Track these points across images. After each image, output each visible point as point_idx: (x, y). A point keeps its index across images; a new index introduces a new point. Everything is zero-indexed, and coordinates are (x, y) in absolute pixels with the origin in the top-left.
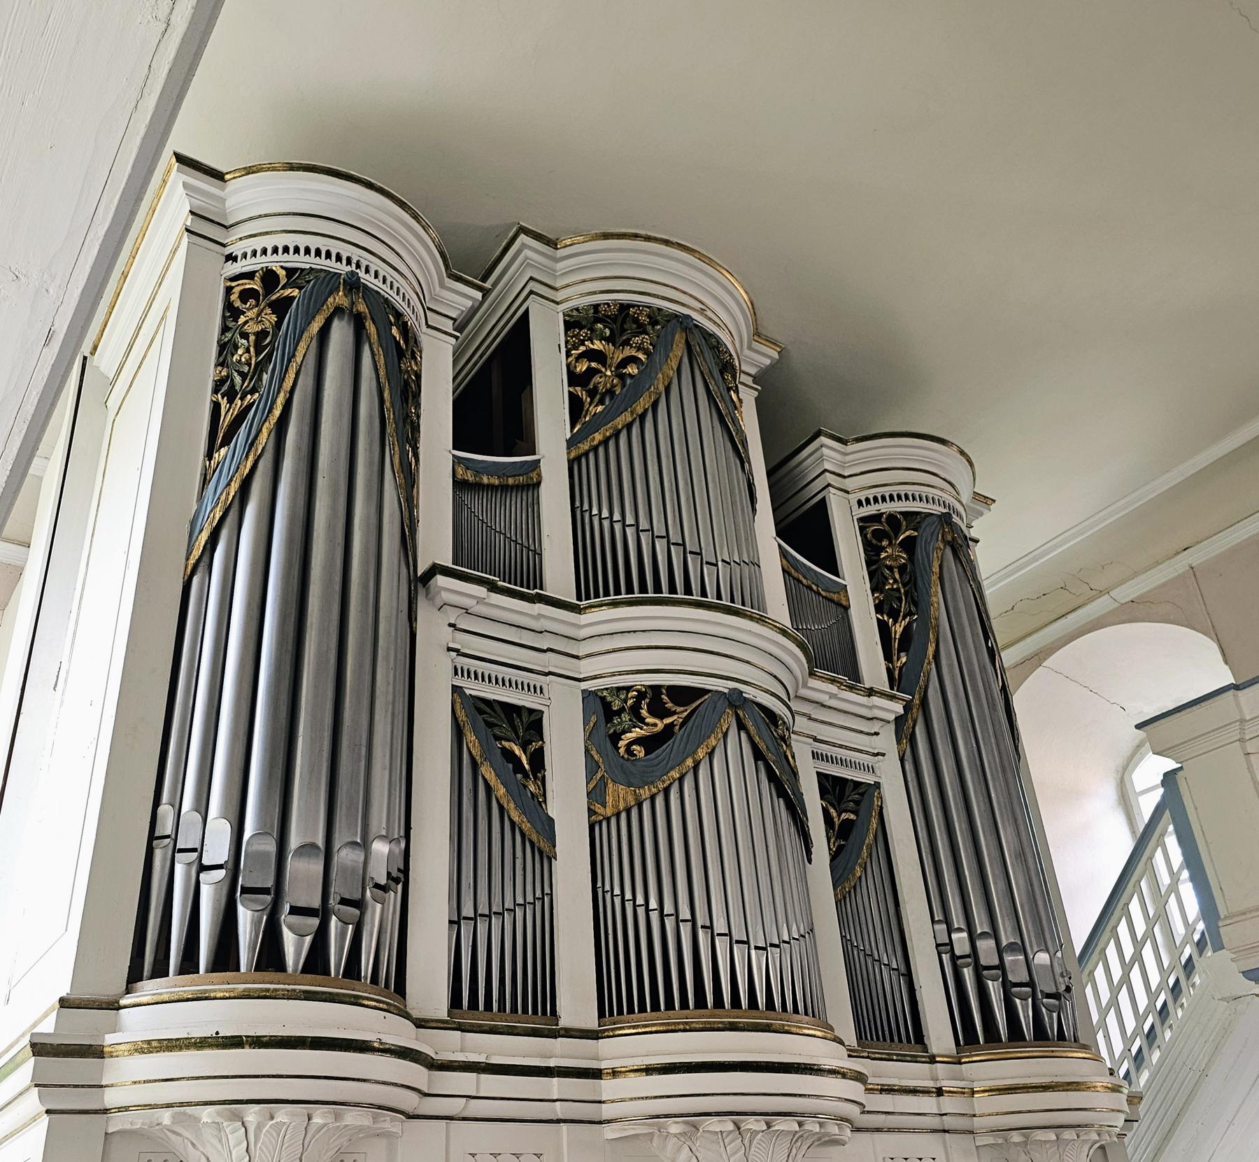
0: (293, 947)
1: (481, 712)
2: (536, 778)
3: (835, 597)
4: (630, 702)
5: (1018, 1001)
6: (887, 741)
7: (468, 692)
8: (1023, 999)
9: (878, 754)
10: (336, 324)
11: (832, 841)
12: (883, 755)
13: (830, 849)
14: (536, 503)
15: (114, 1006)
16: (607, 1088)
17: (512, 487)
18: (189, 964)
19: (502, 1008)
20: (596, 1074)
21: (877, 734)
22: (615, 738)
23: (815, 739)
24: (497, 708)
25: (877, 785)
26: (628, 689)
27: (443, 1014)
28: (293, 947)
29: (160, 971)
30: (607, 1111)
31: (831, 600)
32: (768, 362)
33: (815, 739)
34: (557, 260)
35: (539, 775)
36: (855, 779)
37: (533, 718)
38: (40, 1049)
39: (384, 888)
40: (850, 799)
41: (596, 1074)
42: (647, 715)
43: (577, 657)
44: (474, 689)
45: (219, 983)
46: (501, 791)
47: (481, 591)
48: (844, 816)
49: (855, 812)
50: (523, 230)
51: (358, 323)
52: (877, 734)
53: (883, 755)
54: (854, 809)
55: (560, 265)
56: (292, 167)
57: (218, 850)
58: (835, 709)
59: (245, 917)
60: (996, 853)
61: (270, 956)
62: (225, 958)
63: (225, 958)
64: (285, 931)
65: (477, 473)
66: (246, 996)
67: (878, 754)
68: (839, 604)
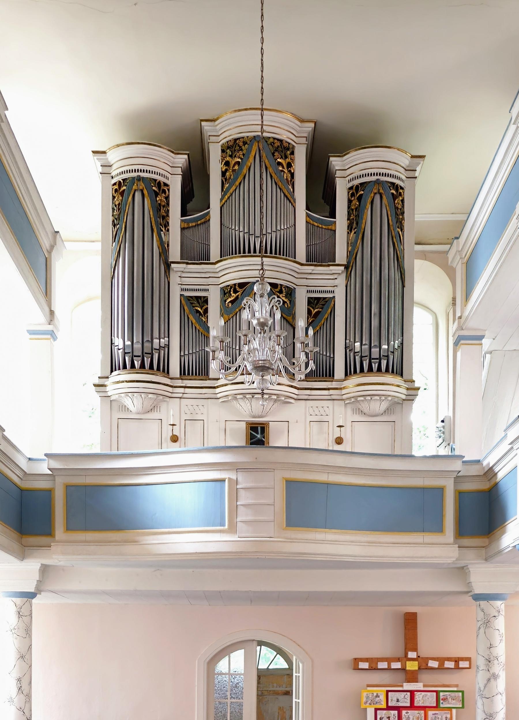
0: (137, 364)
1: (189, 300)
2: (205, 316)
3: (330, 227)
4: (229, 290)
5: (373, 364)
6: (341, 281)
8: (375, 363)
9: (334, 286)
10: (136, 193)
11: (309, 319)
12: (337, 286)
13: (308, 322)
14: (209, 226)
15: (108, 378)
16: (218, 390)
17: (201, 224)
18: (119, 369)
19: (189, 374)
20: (214, 388)
21: (336, 279)
22: (225, 301)
23: (307, 286)
24: (194, 298)
25: (334, 297)
26: (228, 286)
27: (178, 376)
28: (137, 364)
29: (116, 370)
30: (219, 396)
31: (328, 229)
32: (311, 129)
33: (307, 286)
34: (216, 126)
35: (206, 315)
36: (324, 297)
37: (205, 299)
38: (95, 385)
39: (164, 347)
40: (320, 304)
41: (214, 388)
42: (232, 293)
43: (218, 277)
44: (187, 294)
45: (125, 371)
46: (194, 321)
47: (184, 265)
48: (316, 310)
49: (322, 308)
50: (202, 120)
51: (142, 191)
52: (336, 279)
53: (337, 286)
54: (322, 307)
55: (218, 127)
56: (118, 146)
57: (121, 346)
58: (317, 274)
59: (127, 358)
60: (390, 313)
61: (133, 366)
62: (125, 367)
63: (125, 367)
64: (135, 361)
65: (188, 223)
66: (137, 373)
67: (334, 286)
68: (331, 230)
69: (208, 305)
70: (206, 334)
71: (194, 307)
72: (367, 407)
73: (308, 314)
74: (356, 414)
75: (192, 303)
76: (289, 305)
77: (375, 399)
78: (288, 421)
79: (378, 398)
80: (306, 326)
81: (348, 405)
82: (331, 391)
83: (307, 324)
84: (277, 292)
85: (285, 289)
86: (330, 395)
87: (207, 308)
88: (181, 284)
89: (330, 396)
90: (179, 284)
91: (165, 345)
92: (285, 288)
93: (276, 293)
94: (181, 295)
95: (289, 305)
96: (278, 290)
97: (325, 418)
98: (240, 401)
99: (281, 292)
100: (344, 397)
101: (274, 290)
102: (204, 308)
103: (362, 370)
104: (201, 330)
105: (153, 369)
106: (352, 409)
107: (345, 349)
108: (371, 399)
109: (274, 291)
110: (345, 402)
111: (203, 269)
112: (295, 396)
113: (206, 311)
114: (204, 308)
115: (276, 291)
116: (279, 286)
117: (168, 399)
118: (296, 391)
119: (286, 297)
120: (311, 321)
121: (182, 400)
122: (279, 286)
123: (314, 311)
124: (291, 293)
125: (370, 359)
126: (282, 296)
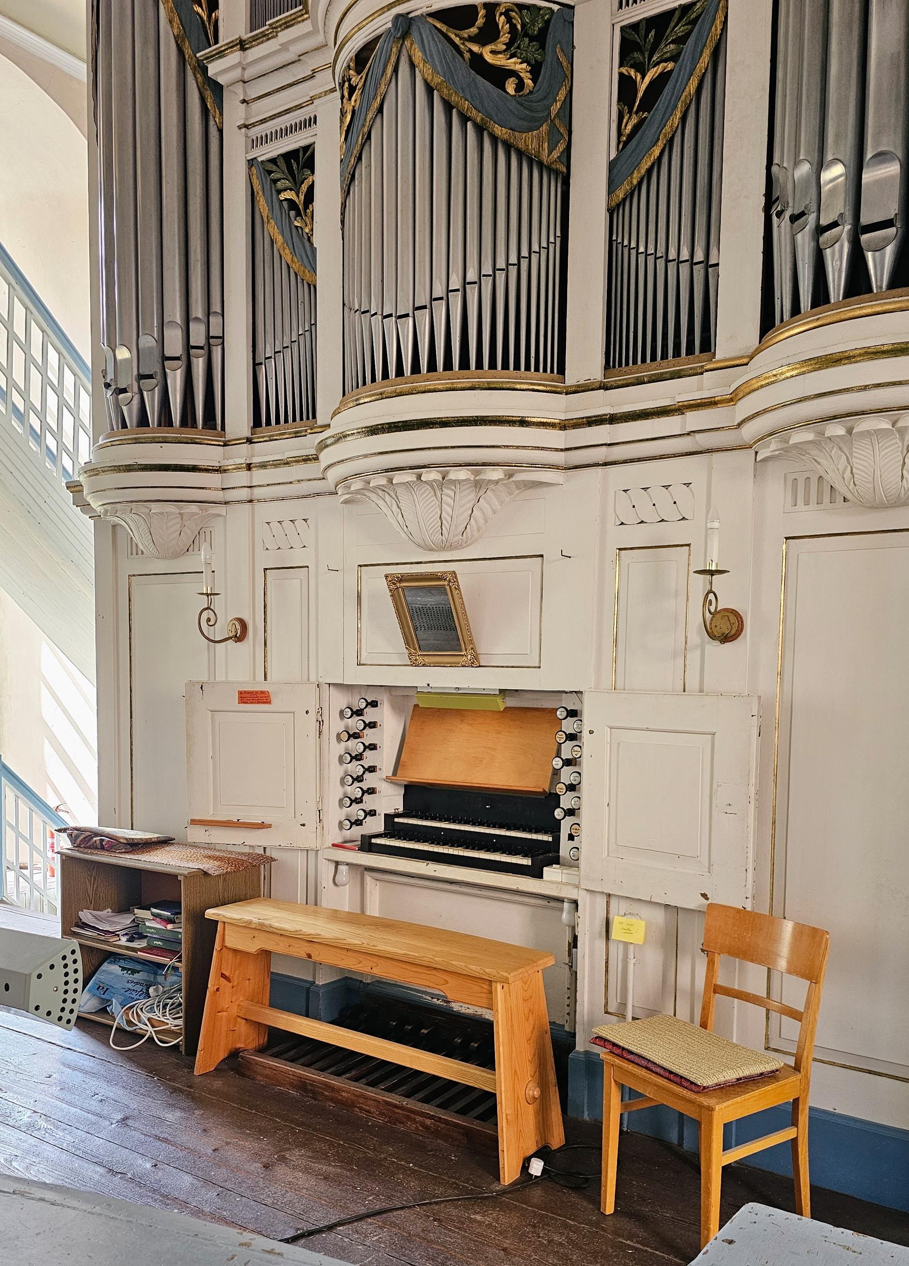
7: (260, 159)
27: (246, 432)
69: (313, 172)
70: (308, 276)
71: (279, 192)
72: (841, 467)
73: (620, 100)
74: (807, 503)
75: (275, 181)
76: (529, 82)
77: (868, 433)
78: (542, 556)
79: (882, 423)
80: (613, 155)
81: (770, 465)
82: (690, 415)
83: (619, 142)
84: (471, 39)
85: (509, 20)
86: (688, 434)
87: (311, 188)
88: (246, 126)
89: (688, 438)
90: (240, 128)
91: (212, 341)
92: (506, 14)
93: (467, 43)
94: (251, 163)
95: (529, 82)
96: (474, 30)
97: (673, 533)
98: (401, 491)
99: (488, 34)
100: (749, 432)
101: (456, 35)
102: (304, 187)
103: (821, 297)
104: (295, 267)
105: (170, 424)
106: (790, 483)
107: (762, 215)
108: (850, 431)
109: (457, 40)
110: (756, 453)
111: (284, 47)
112: (559, 458)
113: (309, 197)
114: (304, 187)
115: (466, 36)
116: (482, 12)
117: (221, 510)
118: (557, 438)
119: (511, 49)
120: (629, 127)
121: (257, 506)
122: (482, 12)
123: (643, 78)
124: (544, 31)
125: (859, 230)
126: (493, 52)
